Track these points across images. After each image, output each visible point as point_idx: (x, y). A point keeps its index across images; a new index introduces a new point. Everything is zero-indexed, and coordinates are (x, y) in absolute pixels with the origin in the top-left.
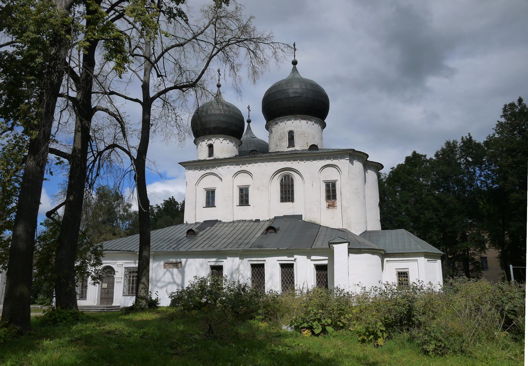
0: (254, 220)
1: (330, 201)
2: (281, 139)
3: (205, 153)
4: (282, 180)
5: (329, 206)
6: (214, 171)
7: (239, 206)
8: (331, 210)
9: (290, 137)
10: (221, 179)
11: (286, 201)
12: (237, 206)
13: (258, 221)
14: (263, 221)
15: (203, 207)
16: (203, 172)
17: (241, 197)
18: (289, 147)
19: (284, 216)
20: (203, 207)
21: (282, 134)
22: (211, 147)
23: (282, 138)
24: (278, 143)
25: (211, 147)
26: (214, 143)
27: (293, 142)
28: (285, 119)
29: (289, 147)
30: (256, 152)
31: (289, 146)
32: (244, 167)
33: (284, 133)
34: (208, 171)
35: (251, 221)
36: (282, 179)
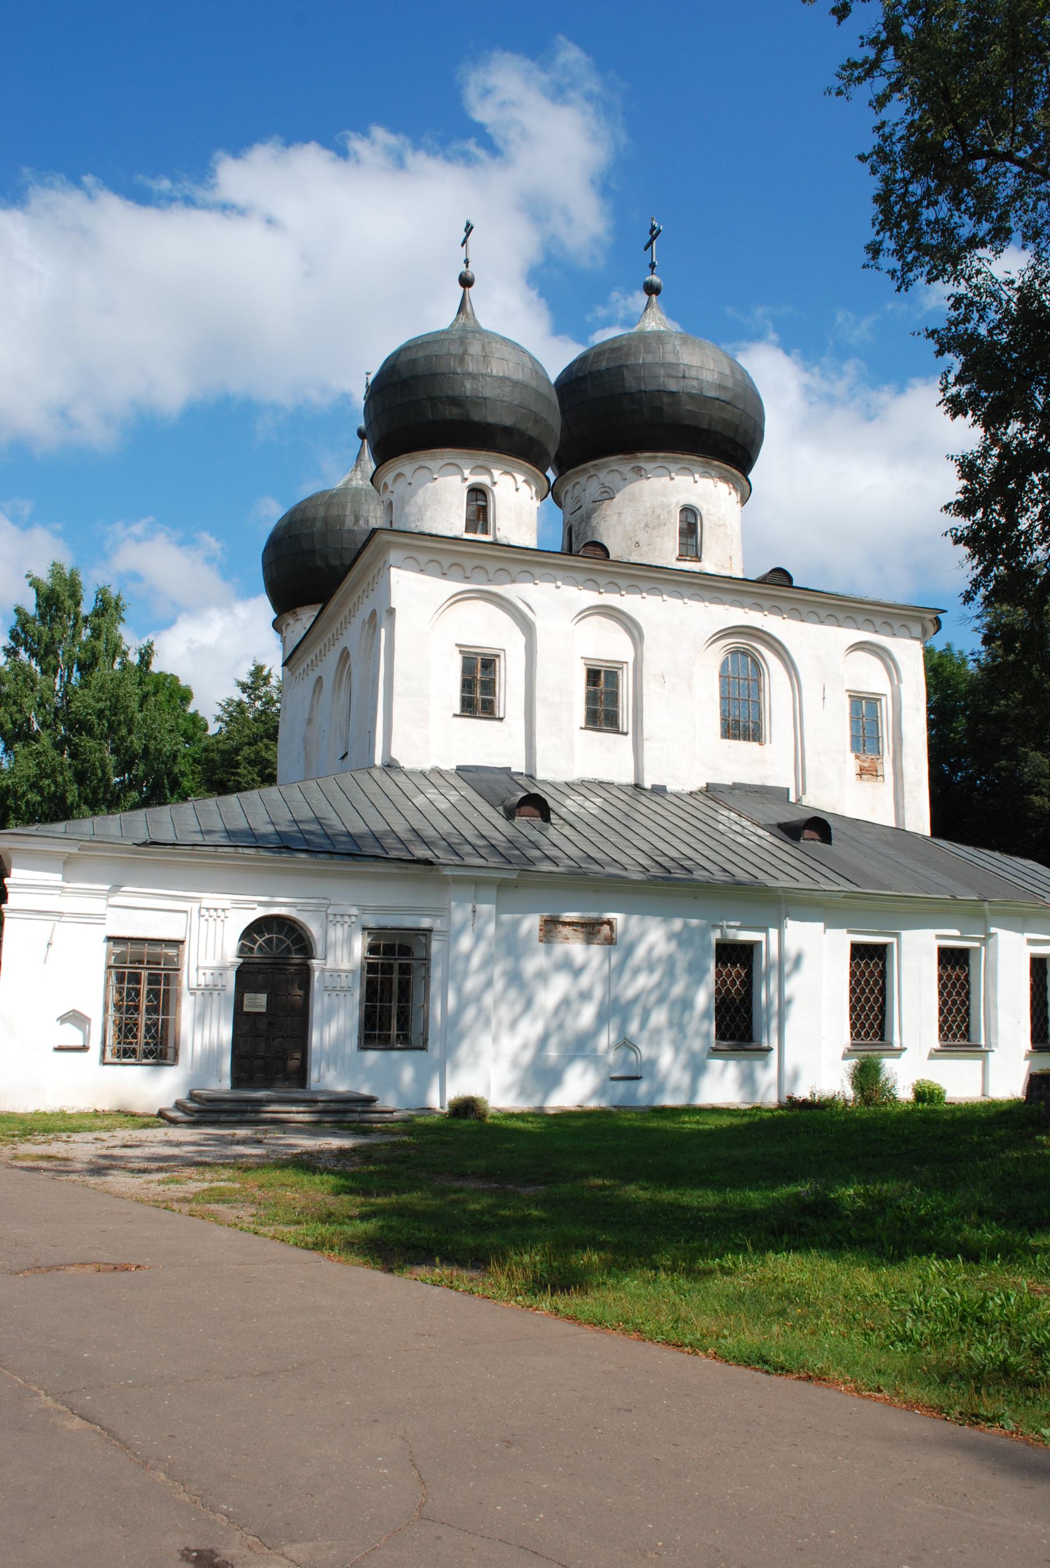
1: (863, 757)
5: (862, 773)
9: (685, 525)
11: (736, 737)
15: (455, 715)
17: (592, 698)
19: (736, 787)
20: (455, 715)
21: (658, 511)
22: (478, 495)
24: (642, 537)
25: (478, 495)
28: (675, 461)
30: (599, 552)
31: (680, 555)
33: (665, 506)
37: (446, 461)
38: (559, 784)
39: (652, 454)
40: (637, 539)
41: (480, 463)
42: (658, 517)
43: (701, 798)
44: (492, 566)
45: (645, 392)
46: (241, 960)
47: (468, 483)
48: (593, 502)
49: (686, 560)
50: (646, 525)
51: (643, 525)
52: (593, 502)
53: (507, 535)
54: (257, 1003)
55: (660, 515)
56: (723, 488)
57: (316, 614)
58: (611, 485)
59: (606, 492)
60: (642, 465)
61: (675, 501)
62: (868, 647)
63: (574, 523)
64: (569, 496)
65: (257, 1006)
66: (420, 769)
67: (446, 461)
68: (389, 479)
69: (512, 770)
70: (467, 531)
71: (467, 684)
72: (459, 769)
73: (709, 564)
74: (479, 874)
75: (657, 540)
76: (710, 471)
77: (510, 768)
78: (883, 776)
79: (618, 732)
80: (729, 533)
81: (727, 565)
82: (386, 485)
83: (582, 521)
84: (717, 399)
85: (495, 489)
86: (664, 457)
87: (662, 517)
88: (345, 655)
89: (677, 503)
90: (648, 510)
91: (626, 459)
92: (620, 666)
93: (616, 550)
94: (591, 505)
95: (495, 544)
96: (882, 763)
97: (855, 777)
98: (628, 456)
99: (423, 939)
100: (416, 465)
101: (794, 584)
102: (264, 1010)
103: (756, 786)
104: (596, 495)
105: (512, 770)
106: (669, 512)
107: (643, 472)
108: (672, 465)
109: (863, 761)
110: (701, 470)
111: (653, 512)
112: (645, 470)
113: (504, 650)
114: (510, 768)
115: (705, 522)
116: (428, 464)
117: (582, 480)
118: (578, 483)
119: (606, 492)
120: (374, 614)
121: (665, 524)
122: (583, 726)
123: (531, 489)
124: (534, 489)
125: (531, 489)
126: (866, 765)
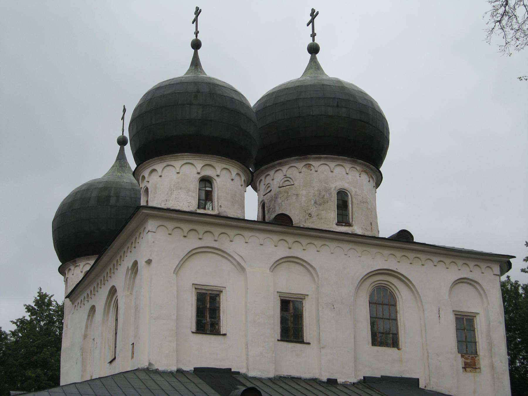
0: (324, 379)
3: (194, 194)
4: (371, 296)
6: (224, 244)
7: (281, 340)
8: (469, 376)
9: (341, 202)
10: (243, 269)
12: (278, 340)
13: (332, 382)
14: (344, 385)
16: (193, 242)
18: (339, 223)
20: (193, 332)
21: (323, 193)
23: (325, 202)
24: (313, 210)
26: (218, 176)
27: (347, 215)
28: (333, 159)
29: (339, 223)
32: (297, 251)
33: (327, 190)
34: (208, 241)
35: (315, 381)
36: (374, 290)
37: (185, 161)
38: (264, 379)
40: (310, 212)
41: (207, 162)
42: (323, 197)
43: (360, 387)
44: (217, 231)
45: (313, 116)
47: (199, 176)
48: (280, 187)
49: (342, 225)
50: (315, 203)
51: (313, 202)
52: (280, 187)
53: (226, 210)
55: (324, 196)
56: (365, 177)
57: (92, 262)
58: (291, 176)
60: (311, 163)
61: (334, 186)
62: (466, 281)
63: (266, 201)
64: (262, 183)
66: (169, 370)
67: (185, 161)
68: (146, 173)
69: (232, 370)
70: (199, 208)
71: (200, 312)
72: (197, 370)
73: (357, 229)
75: (323, 212)
76: (356, 167)
77: (231, 369)
78: (479, 368)
79: (302, 342)
80: (369, 207)
81: (369, 228)
82: (144, 177)
83: (272, 200)
84: (360, 120)
85: (218, 179)
86: (326, 158)
87: (326, 197)
88: (113, 291)
89: (335, 187)
90: (316, 193)
91: (301, 159)
92: (304, 298)
93: (297, 218)
94: (278, 189)
95: (218, 216)
96: (479, 360)
97: (461, 370)
98: (302, 157)
100: (165, 164)
101: (414, 241)
103: (396, 377)
104: (281, 183)
105: (232, 370)
106: (330, 194)
107: (312, 167)
108: (331, 163)
109: (467, 359)
110: (350, 166)
111: (320, 194)
112: (314, 166)
113: (225, 288)
114: (231, 369)
115: (354, 200)
116: (173, 163)
117: (272, 173)
118: (268, 175)
120: (136, 263)
121: (328, 202)
122: (279, 339)
123: (241, 180)
124: (243, 178)
125: (241, 180)
126: (468, 361)
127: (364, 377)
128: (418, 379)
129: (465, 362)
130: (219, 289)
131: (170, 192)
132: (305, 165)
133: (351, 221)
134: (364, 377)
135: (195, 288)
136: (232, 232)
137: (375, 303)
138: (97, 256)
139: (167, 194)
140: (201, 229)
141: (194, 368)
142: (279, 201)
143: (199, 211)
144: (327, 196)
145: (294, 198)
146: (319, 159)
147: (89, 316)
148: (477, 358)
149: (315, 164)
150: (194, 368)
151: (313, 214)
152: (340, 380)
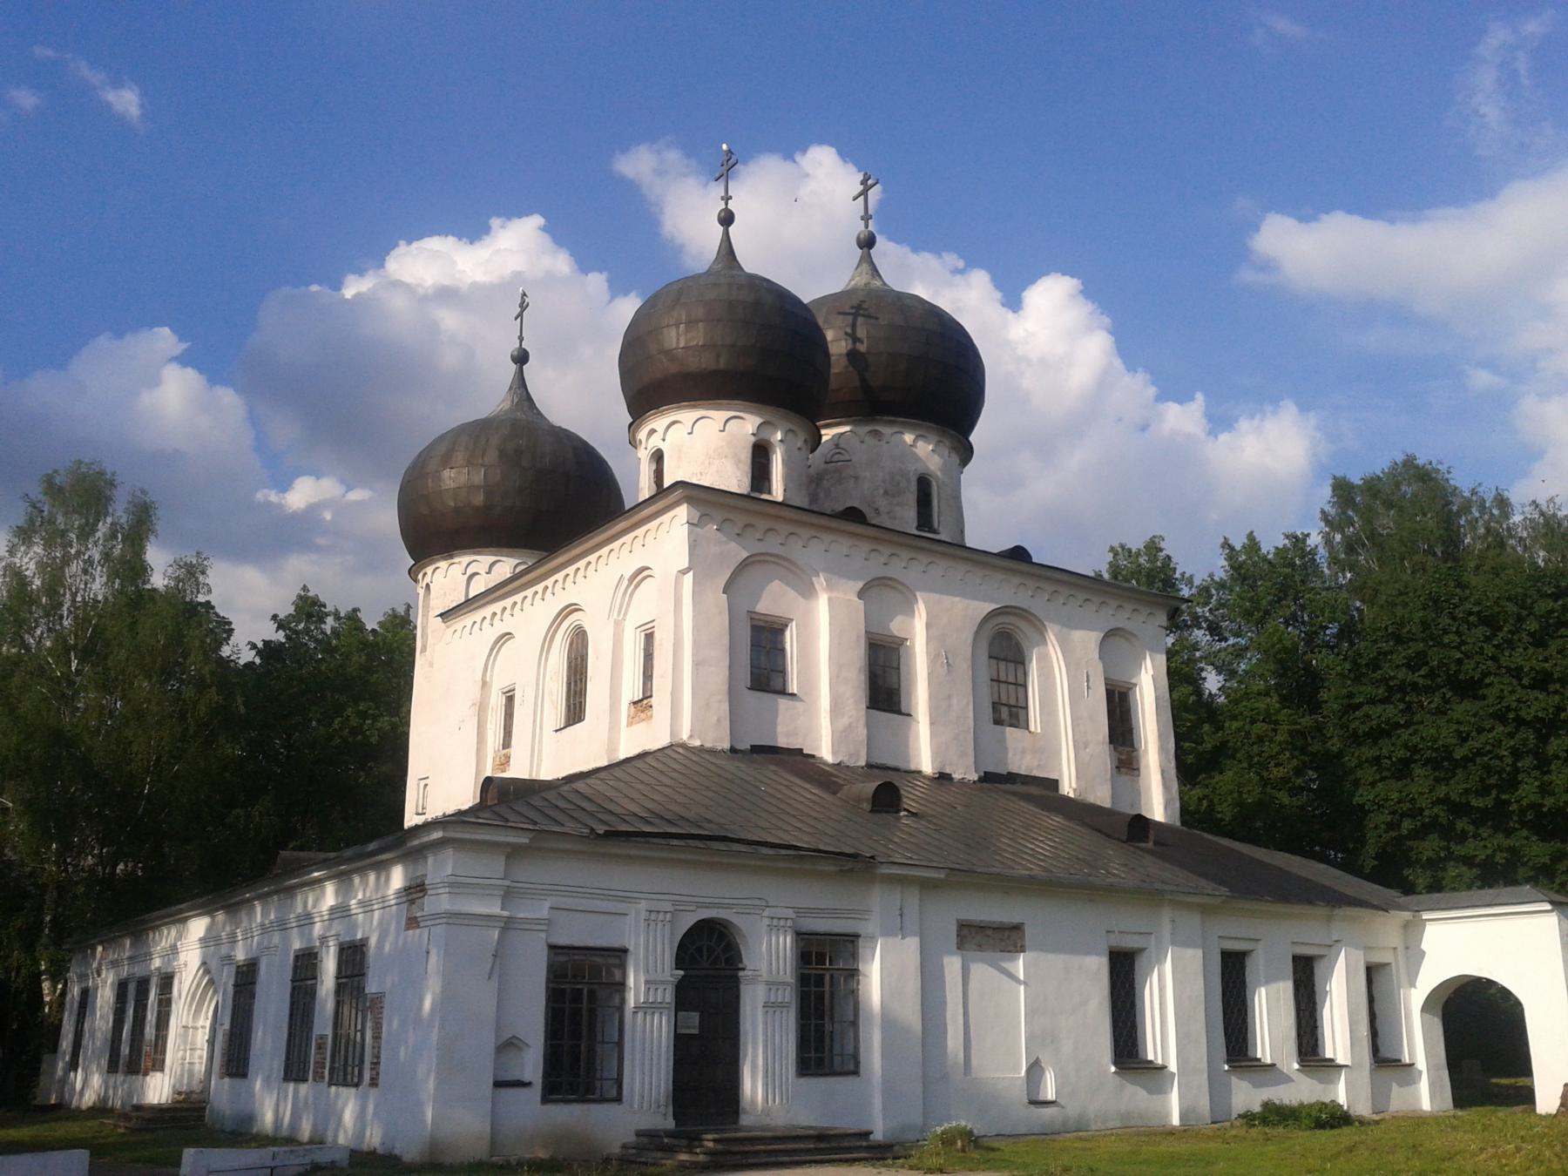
2: (892, 492)
4: (991, 644)
29: (919, 528)
34: (772, 545)
39: (893, 418)
46: (682, 973)
48: (826, 463)
50: (886, 493)
51: (882, 491)
52: (826, 463)
54: (693, 1019)
59: (839, 453)
65: (689, 1027)
69: (805, 752)
74: (911, 873)
77: (801, 750)
78: (1138, 769)
79: (899, 712)
94: (823, 466)
99: (850, 946)
102: (695, 1031)
104: (829, 456)
114: (801, 750)
119: (839, 453)
121: (904, 492)
127: (985, 773)
128: (1057, 781)
129: (1119, 759)
130: (783, 621)
131: (707, 462)
132: (870, 432)
133: (936, 525)
134: (985, 773)
135: (751, 619)
136: (806, 533)
137: (995, 658)
138: (546, 554)
139: (703, 463)
140: (762, 524)
141: (752, 746)
142: (825, 484)
143: (753, 495)
144: (903, 484)
145: (852, 482)
146: (892, 423)
147: (492, 650)
148: (1134, 754)
149: (887, 430)
150: (752, 746)
151: (881, 509)
152: (957, 776)
